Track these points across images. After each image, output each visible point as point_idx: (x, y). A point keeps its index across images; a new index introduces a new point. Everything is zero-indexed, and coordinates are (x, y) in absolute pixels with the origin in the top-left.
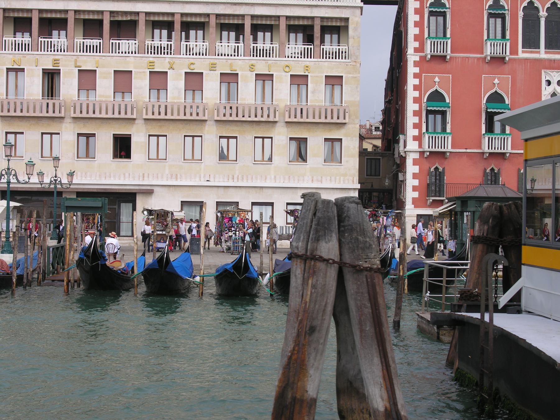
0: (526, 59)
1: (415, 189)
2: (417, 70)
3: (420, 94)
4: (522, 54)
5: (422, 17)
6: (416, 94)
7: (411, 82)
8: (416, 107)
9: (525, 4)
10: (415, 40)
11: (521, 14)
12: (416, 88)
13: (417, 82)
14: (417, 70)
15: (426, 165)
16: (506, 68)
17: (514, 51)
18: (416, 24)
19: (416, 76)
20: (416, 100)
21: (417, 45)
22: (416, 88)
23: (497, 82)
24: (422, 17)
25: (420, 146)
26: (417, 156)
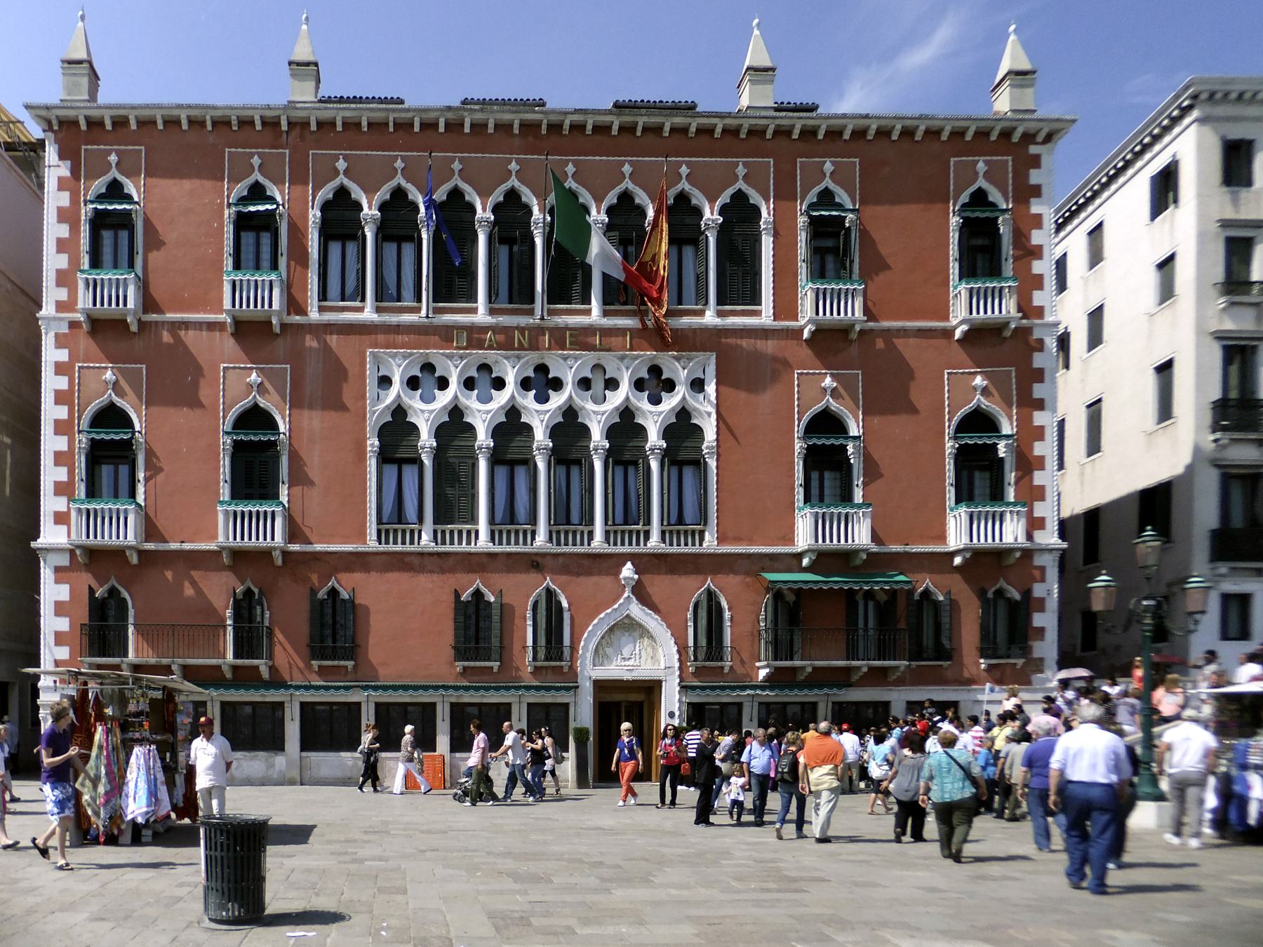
1: (60, 639)
2: (63, 355)
3: (71, 412)
5: (75, 228)
6: (62, 412)
7: (51, 383)
8: (62, 444)
9: (327, 192)
10: (59, 283)
11: (314, 215)
12: (60, 398)
13: (62, 383)
14: (63, 355)
15: (87, 579)
16: (281, 346)
17: (294, 305)
18: (61, 245)
19: (60, 369)
20: (61, 428)
21: (63, 294)
22: (60, 398)
24: (75, 228)
25: (69, 535)
26: (64, 561)
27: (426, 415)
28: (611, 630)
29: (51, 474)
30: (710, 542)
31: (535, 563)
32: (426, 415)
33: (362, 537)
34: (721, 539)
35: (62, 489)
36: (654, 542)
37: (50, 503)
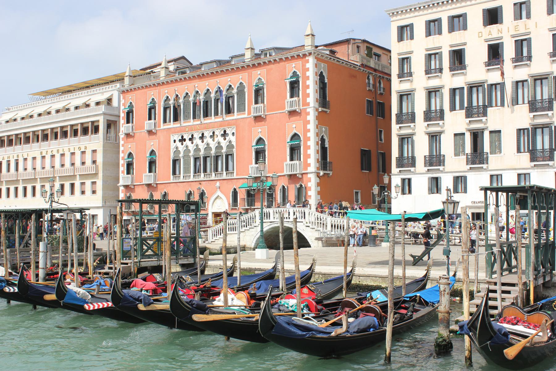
0: (164, 129)
4: (163, 126)
7: (121, 148)
12: (123, 152)
17: (159, 126)
20: (123, 158)
22: (123, 152)
23: (152, 144)
27: (181, 148)
28: (216, 199)
29: (121, 169)
30: (235, 176)
31: (200, 182)
32: (181, 148)
33: (170, 179)
34: (237, 175)
35: (123, 172)
36: (224, 176)
37: (121, 175)
